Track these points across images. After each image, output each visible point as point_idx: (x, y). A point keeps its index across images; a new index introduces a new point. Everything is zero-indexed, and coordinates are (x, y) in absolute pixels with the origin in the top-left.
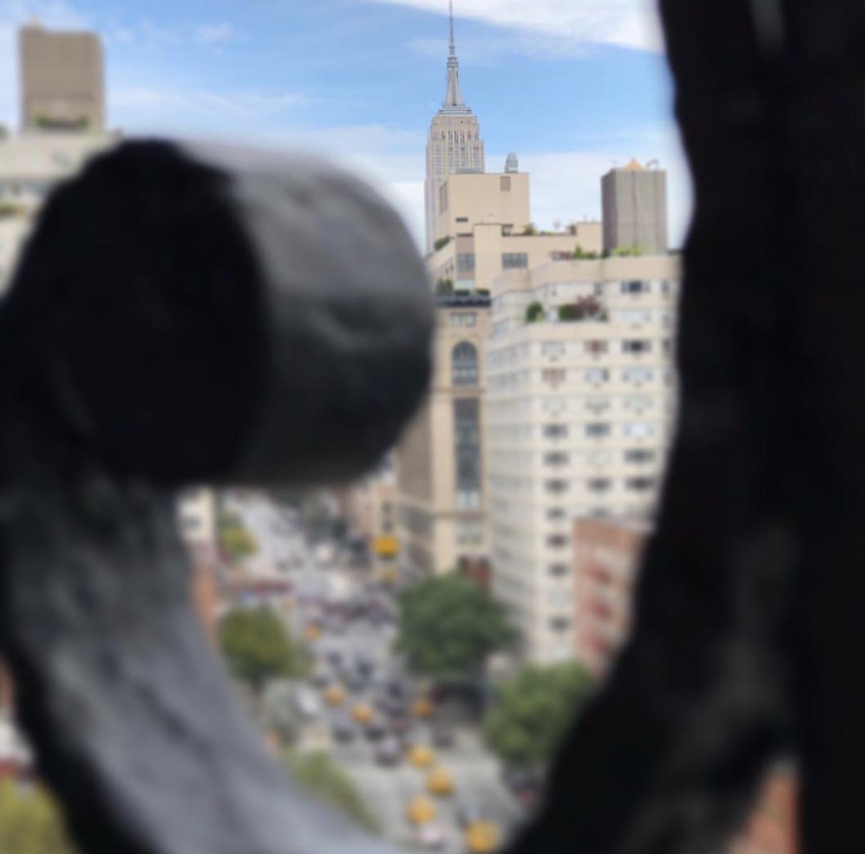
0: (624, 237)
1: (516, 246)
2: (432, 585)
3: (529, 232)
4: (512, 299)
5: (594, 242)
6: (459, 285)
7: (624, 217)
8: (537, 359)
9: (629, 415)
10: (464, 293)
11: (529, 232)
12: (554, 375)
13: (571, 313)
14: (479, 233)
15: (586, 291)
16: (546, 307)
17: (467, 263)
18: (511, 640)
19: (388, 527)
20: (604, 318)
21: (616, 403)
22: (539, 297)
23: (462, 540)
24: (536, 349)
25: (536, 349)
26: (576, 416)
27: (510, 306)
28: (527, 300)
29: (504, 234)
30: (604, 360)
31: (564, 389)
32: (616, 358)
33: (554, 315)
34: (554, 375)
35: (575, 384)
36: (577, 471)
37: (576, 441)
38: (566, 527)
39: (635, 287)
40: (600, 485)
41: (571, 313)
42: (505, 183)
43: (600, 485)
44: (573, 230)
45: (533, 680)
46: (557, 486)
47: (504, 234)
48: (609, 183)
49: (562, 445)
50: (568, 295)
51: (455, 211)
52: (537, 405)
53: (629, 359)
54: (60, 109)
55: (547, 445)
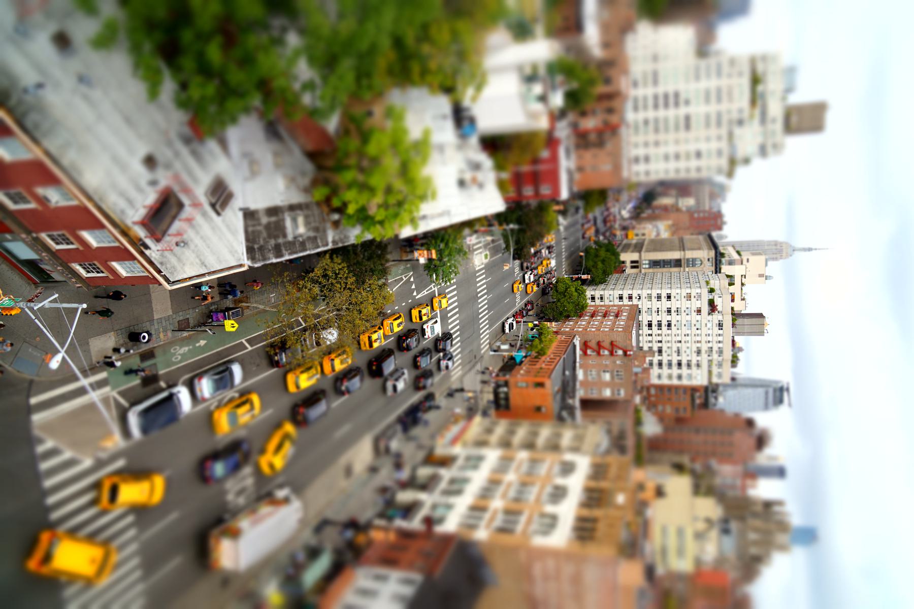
1: (737, 281)
2: (617, 255)
3: (743, 284)
5: (739, 306)
6: (723, 260)
7: (747, 321)
12: (689, 297)
13: (711, 303)
14: (743, 267)
15: (719, 308)
17: (731, 263)
20: (709, 314)
24: (698, 291)
25: (698, 291)
26: (673, 304)
28: (716, 287)
31: (684, 300)
34: (689, 297)
35: (685, 304)
36: (656, 304)
37: (665, 304)
38: (635, 301)
39: (720, 325)
41: (711, 303)
42: (761, 276)
46: (650, 297)
48: (760, 316)
49: (664, 299)
50: (718, 302)
51: (752, 258)
52: (678, 291)
55: (664, 295)
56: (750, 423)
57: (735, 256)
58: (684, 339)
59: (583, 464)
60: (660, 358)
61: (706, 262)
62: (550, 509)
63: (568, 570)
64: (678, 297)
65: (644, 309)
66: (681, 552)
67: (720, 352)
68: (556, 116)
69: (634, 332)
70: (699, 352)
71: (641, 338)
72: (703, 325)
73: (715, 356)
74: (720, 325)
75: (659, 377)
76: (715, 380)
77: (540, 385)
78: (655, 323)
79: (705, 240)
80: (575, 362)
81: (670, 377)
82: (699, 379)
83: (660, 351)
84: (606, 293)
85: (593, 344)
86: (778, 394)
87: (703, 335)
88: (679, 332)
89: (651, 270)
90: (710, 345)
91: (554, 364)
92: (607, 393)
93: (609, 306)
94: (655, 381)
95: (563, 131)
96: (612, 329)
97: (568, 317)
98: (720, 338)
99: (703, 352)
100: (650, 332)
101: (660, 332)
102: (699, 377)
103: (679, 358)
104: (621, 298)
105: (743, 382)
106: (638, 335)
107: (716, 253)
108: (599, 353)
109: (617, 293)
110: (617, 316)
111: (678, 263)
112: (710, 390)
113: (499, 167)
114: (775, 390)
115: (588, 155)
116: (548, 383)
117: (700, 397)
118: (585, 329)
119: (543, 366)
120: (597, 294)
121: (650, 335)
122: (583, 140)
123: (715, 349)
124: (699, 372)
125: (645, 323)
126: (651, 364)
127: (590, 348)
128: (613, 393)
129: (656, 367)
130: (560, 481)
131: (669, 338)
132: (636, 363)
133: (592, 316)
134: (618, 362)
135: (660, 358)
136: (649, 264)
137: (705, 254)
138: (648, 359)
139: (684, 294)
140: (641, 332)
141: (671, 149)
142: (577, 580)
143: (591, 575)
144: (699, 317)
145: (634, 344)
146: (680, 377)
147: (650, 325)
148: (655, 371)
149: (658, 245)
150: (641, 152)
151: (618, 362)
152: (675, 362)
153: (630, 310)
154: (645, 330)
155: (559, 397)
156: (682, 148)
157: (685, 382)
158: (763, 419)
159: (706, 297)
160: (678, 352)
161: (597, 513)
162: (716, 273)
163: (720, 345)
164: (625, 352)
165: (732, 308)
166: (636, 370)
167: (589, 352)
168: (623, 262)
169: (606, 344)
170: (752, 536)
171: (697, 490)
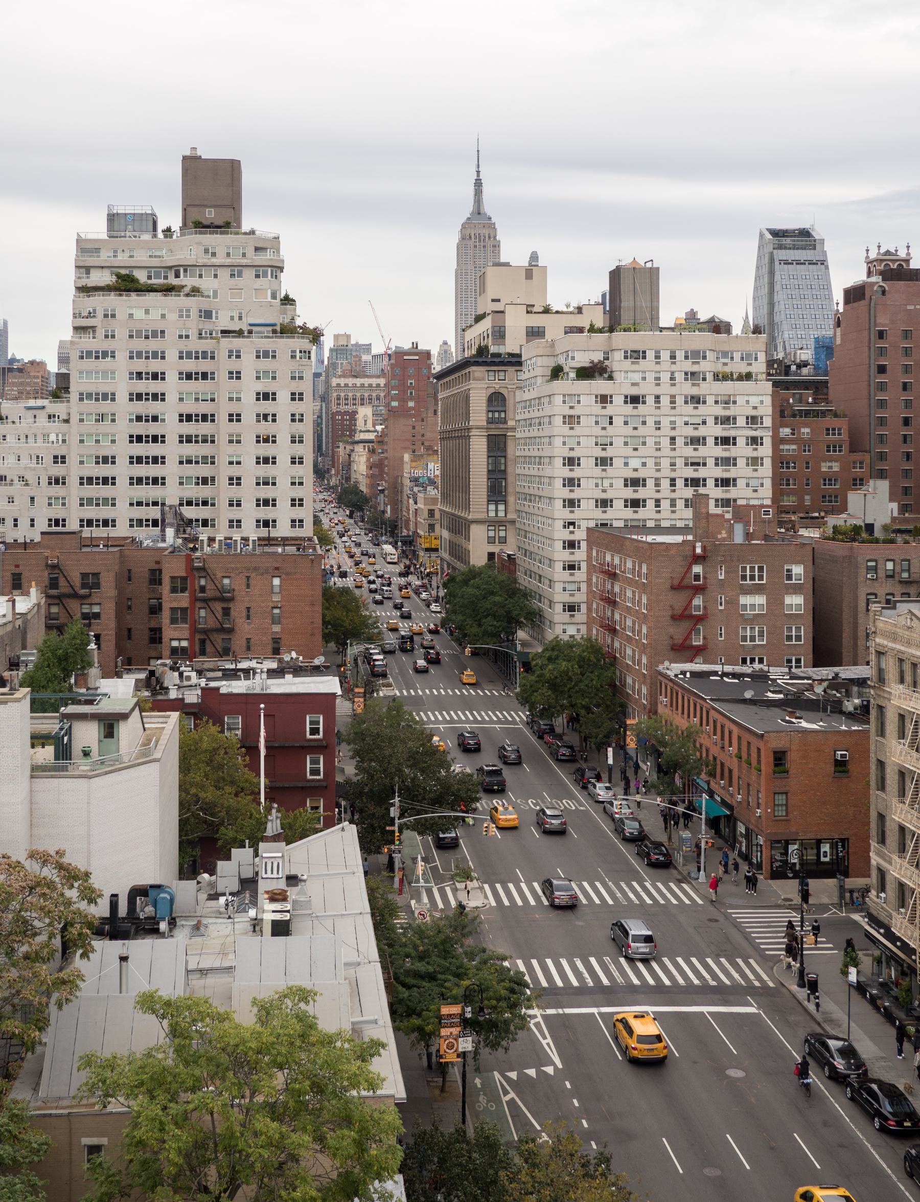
0: (626, 317)
1: (537, 321)
2: (473, 573)
3: (547, 311)
4: (540, 361)
6: (493, 349)
8: (559, 408)
9: (628, 451)
10: (498, 355)
11: (547, 311)
12: (571, 420)
13: (586, 373)
14: (509, 310)
15: (598, 357)
16: (566, 369)
17: (500, 334)
18: (535, 619)
19: (432, 527)
20: (611, 378)
21: (618, 442)
22: (561, 361)
23: (491, 540)
24: (558, 400)
25: (558, 400)
26: (587, 450)
27: (537, 364)
28: (552, 363)
29: (528, 312)
30: (610, 410)
31: (578, 430)
32: (618, 407)
33: (572, 375)
34: (571, 420)
35: (587, 426)
36: (587, 492)
37: (587, 469)
38: (580, 535)
39: (637, 355)
40: (604, 503)
41: (586, 373)
42: (529, 274)
43: (604, 503)
44: (580, 310)
45: (557, 650)
47: (528, 312)
48: (616, 275)
49: (577, 473)
50: (583, 359)
51: (491, 293)
53: (629, 409)
54: (210, 215)
56: (854, 295)
57: (486, 325)
58: (666, 430)
60: (711, 483)
61: (497, 386)
64: (572, 443)
67: (696, 355)
68: (155, 697)
69: (650, 539)
70: (696, 400)
71: (664, 524)
73: (705, 366)
74: (637, 355)
79: (447, 386)
81: (755, 462)
82: (759, 398)
83: (695, 482)
84: (560, 597)
85: (678, 632)
86: (788, 241)
88: (650, 441)
89: (511, 499)
90: (680, 377)
91: (729, 725)
92: (795, 601)
93: (589, 591)
94: (766, 494)
95: (187, 684)
96: (643, 588)
99: (695, 391)
100: (650, 504)
101: (650, 483)
102: (754, 400)
103: (710, 441)
104: (572, 567)
105: (765, 311)
106: (658, 530)
107: (477, 364)
108: (699, 619)
109: (559, 574)
110: (613, 576)
111: (497, 445)
112: (782, 375)
113: (256, 838)
114: (781, 247)
115: (244, 628)
118: (643, 649)
119: (733, 750)
120: (558, 615)
121: (658, 503)
122: (213, 642)
123: (688, 366)
124: (740, 400)
125: (629, 513)
126: (726, 503)
127: (688, 637)
128: (796, 589)
129: (732, 493)
131: (665, 463)
132: (724, 534)
133: (613, 631)
135: (711, 483)
136: (497, 503)
137: (479, 386)
138: (713, 509)
139: (565, 430)
140: (650, 524)
141: (250, 450)
145: (679, 539)
147: (635, 504)
148: (740, 493)
149: (455, 482)
150: (249, 514)
153: (599, 545)
154: (647, 513)
156: (249, 427)
158: (846, 271)
159: (568, 385)
160: (696, 441)
162: (520, 364)
163: (680, 355)
164: (697, 559)
166: (739, 538)
167: (697, 642)
168: (491, 556)
169: (678, 601)
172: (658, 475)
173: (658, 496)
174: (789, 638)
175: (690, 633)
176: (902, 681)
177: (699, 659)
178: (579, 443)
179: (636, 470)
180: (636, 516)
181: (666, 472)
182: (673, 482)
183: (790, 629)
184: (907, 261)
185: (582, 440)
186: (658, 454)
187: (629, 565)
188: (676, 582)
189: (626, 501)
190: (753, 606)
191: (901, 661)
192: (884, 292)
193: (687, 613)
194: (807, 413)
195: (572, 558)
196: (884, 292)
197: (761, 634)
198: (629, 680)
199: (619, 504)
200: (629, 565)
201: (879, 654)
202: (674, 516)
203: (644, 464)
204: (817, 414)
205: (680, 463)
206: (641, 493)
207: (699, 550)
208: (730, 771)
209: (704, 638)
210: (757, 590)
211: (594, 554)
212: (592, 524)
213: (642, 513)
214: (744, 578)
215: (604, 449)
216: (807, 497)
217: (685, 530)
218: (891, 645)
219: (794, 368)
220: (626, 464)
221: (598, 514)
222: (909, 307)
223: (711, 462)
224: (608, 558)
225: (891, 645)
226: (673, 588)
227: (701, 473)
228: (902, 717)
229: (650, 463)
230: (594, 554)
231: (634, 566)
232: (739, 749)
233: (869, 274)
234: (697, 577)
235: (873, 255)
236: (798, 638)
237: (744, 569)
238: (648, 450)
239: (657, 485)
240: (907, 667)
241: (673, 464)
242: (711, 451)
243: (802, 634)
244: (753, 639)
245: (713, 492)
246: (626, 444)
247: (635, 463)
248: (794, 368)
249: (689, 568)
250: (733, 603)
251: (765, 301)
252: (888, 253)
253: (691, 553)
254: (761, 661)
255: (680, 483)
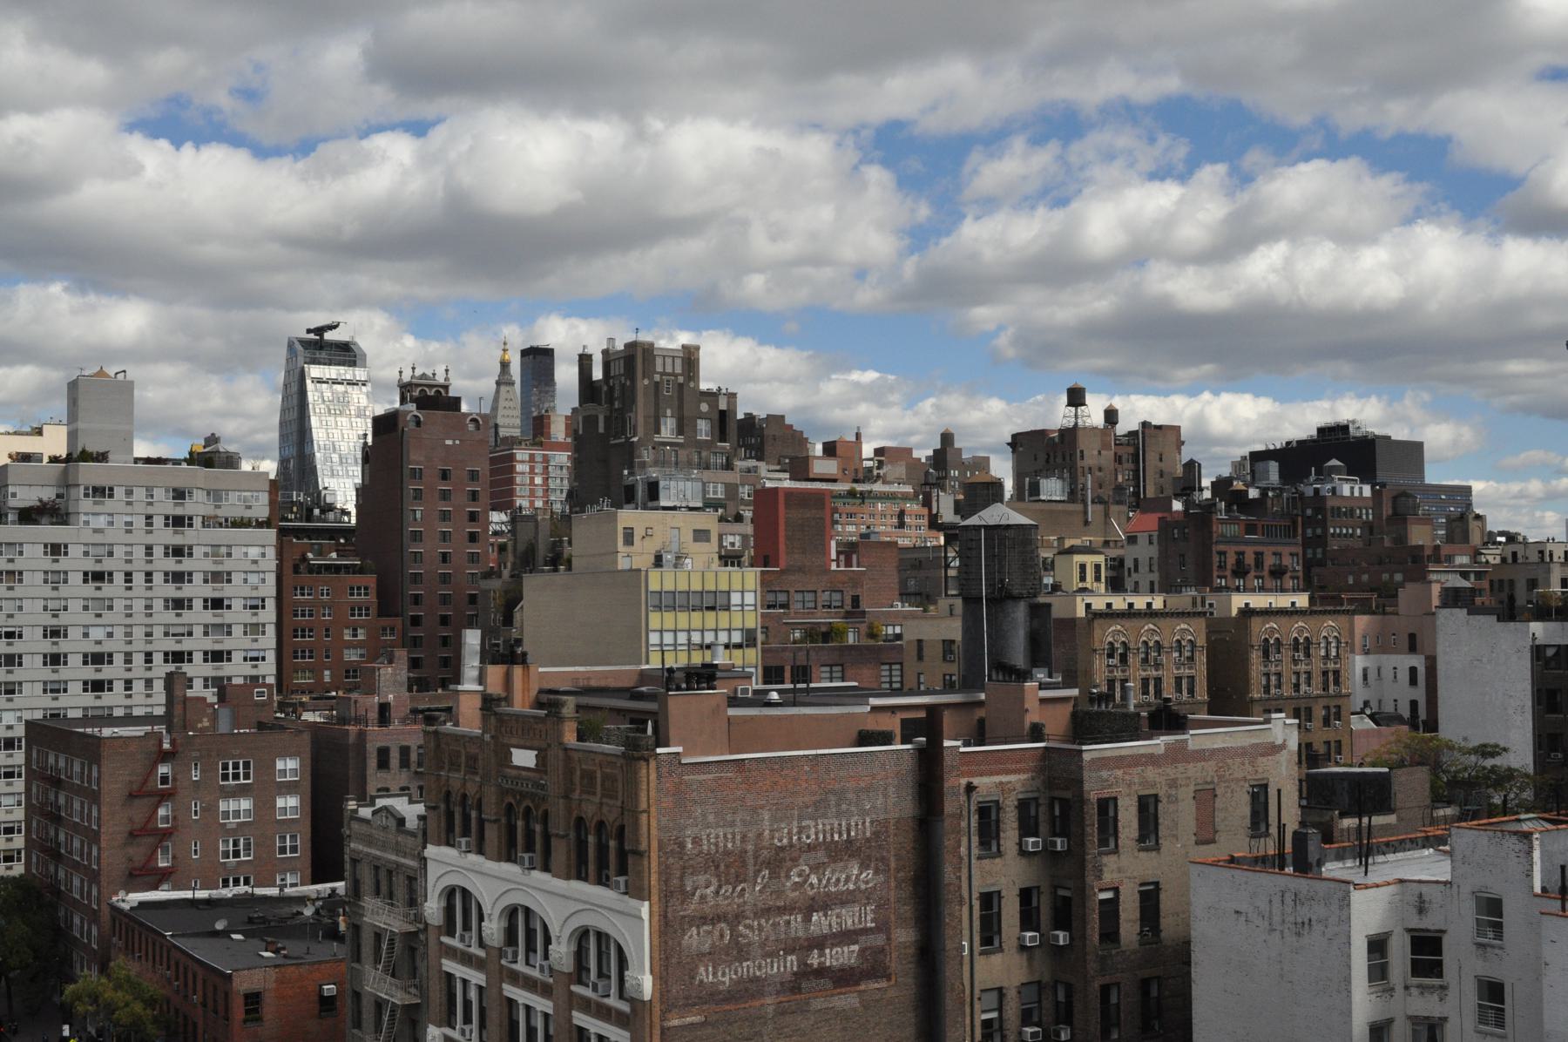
9: (89, 618)
15: (48, 494)
21: (75, 606)
31: (19, 591)
39: (101, 492)
59: (447, 865)
60: (198, 657)
62: (562, 952)
63: (706, 890)
65: (47, 702)
66: (715, 603)
69: (107, 732)
71: (137, 712)
72: (98, 538)
75: (253, 655)
76: (261, 510)
77: (253, 1000)
78: (90, 673)
80: (193, 903)
81: (255, 629)
82: (256, 555)
83: (178, 657)
85: (138, 852)
87: (129, 539)
88: (119, 605)
90: (158, 522)
94: (268, 669)
97: (60, 932)
98: (139, 494)
99: (178, 540)
100: (119, 686)
101: (119, 659)
102: (254, 552)
103: (198, 604)
106: (128, 720)
108: (167, 834)
110: (56, 783)
116: (245, 983)
117: (321, 553)
121: (128, 684)
125: (89, 699)
127: (152, 856)
128: (289, 789)
129: (226, 669)
130: (493, 928)
131: (139, 633)
134: (195, 776)
135: (198, 657)
138: (197, 690)
140: (119, 712)
142: (730, 867)
143: (710, 832)
144: (75, 551)
146: (256, 606)
147: (98, 686)
148: (236, 670)
151: (195, 776)
152: (209, 617)
155: (293, 947)
157: (269, 589)
161: (559, 825)
164: (165, 757)
165: (54, 460)
166: (224, 726)
170: (668, 430)
171: (557, 560)
172: (128, 648)
173: (128, 675)
174: (283, 850)
175: (154, 852)
176: (377, 893)
177: (165, 887)
178: (20, 608)
179: (99, 642)
180: (98, 703)
181: (139, 645)
182: (149, 657)
183: (283, 839)
184: (446, 387)
185: (25, 603)
186: (129, 621)
187: (77, 768)
188: (135, 787)
189: (85, 683)
190: (237, 813)
191: (377, 868)
192: (418, 423)
193: (150, 826)
194: (328, 568)
195: (10, 762)
196: (418, 423)
197: (247, 847)
198: (77, 920)
199: (75, 688)
200: (77, 768)
201: (355, 861)
202: (149, 701)
203: (110, 635)
204: (337, 569)
205: (158, 632)
206: (106, 672)
207: (166, 746)
208: (195, 1025)
209: (174, 857)
210: (242, 792)
211: (34, 755)
212: (38, 715)
213: (107, 699)
214: (225, 777)
215: (55, 616)
216: (327, 673)
217: (148, 719)
218: (367, 850)
219: (317, 512)
220: (86, 635)
221: (47, 702)
222: (449, 442)
223: (198, 631)
224: (51, 760)
225: (367, 850)
226: (131, 796)
227: (186, 645)
228: (378, 936)
229: (119, 633)
230: (34, 755)
231: (83, 769)
232: (205, 994)
233: (403, 401)
234: (164, 780)
235: (407, 378)
236: (294, 849)
237: (225, 767)
238: (116, 616)
239: (128, 660)
240: (383, 875)
241: (149, 634)
242: (199, 615)
243: (298, 845)
244: (236, 854)
245: (198, 669)
246: (86, 608)
247: (97, 633)
248: (317, 512)
249: (154, 767)
250: (210, 809)
251: (294, 427)
252: (424, 376)
253: (155, 749)
254: (247, 882)
255: (158, 658)
